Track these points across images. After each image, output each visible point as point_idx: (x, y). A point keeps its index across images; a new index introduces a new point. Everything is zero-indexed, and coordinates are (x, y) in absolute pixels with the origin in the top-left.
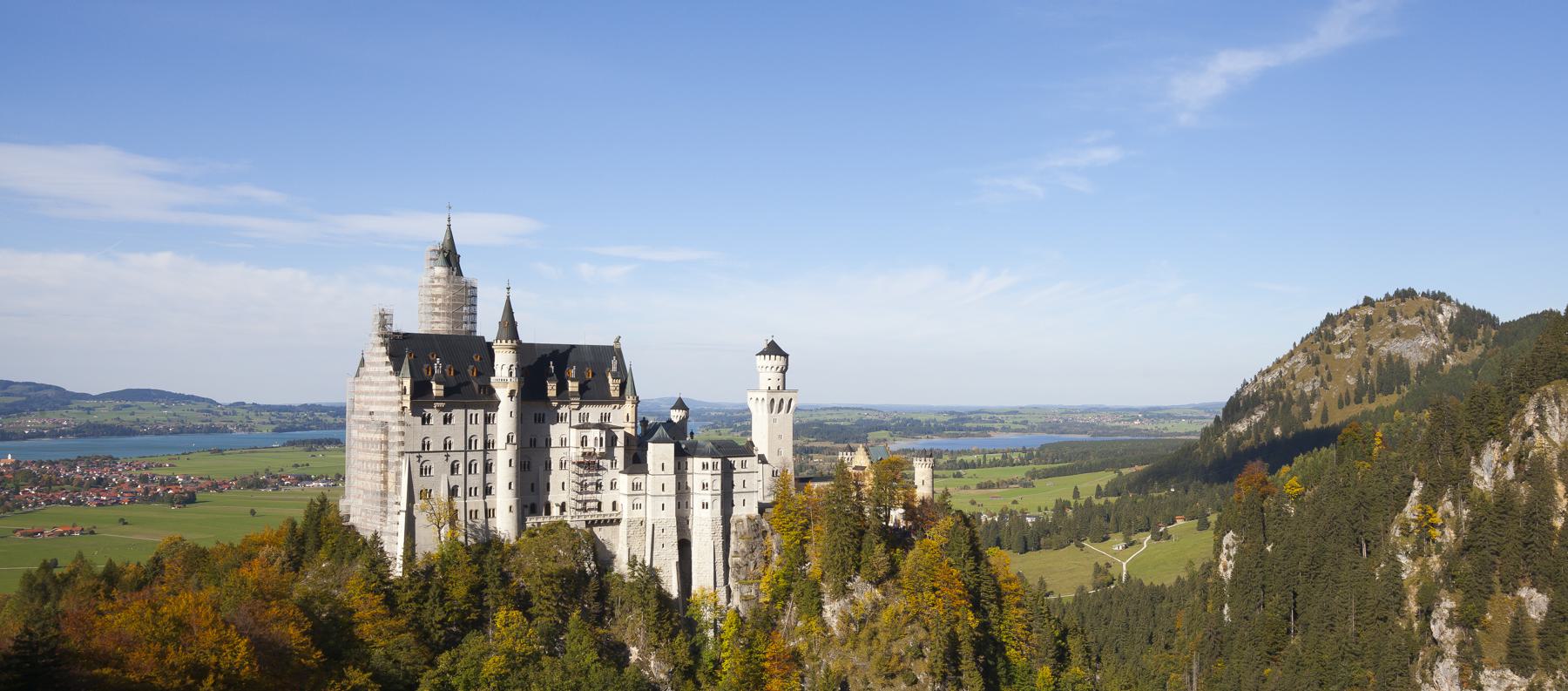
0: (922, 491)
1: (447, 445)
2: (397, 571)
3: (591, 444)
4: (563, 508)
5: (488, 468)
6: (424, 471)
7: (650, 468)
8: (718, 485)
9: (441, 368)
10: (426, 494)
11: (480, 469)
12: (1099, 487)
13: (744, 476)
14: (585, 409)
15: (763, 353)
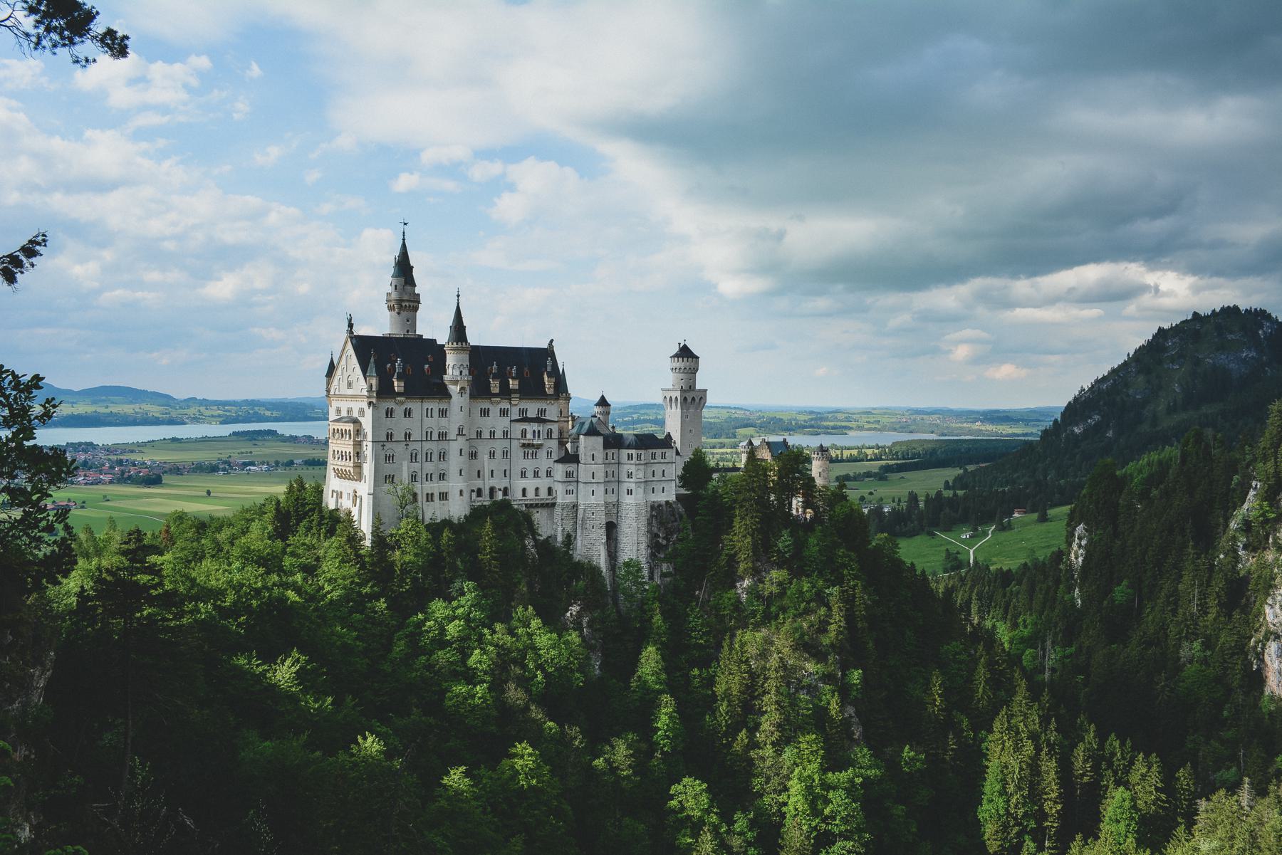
0: (819, 482)
1: (408, 436)
2: (368, 543)
3: (529, 436)
4: (505, 491)
5: (443, 456)
6: (390, 458)
7: (582, 458)
8: (641, 475)
9: (401, 364)
10: (390, 479)
11: (435, 457)
12: (947, 482)
13: (664, 467)
14: (525, 404)
15: (676, 356)
